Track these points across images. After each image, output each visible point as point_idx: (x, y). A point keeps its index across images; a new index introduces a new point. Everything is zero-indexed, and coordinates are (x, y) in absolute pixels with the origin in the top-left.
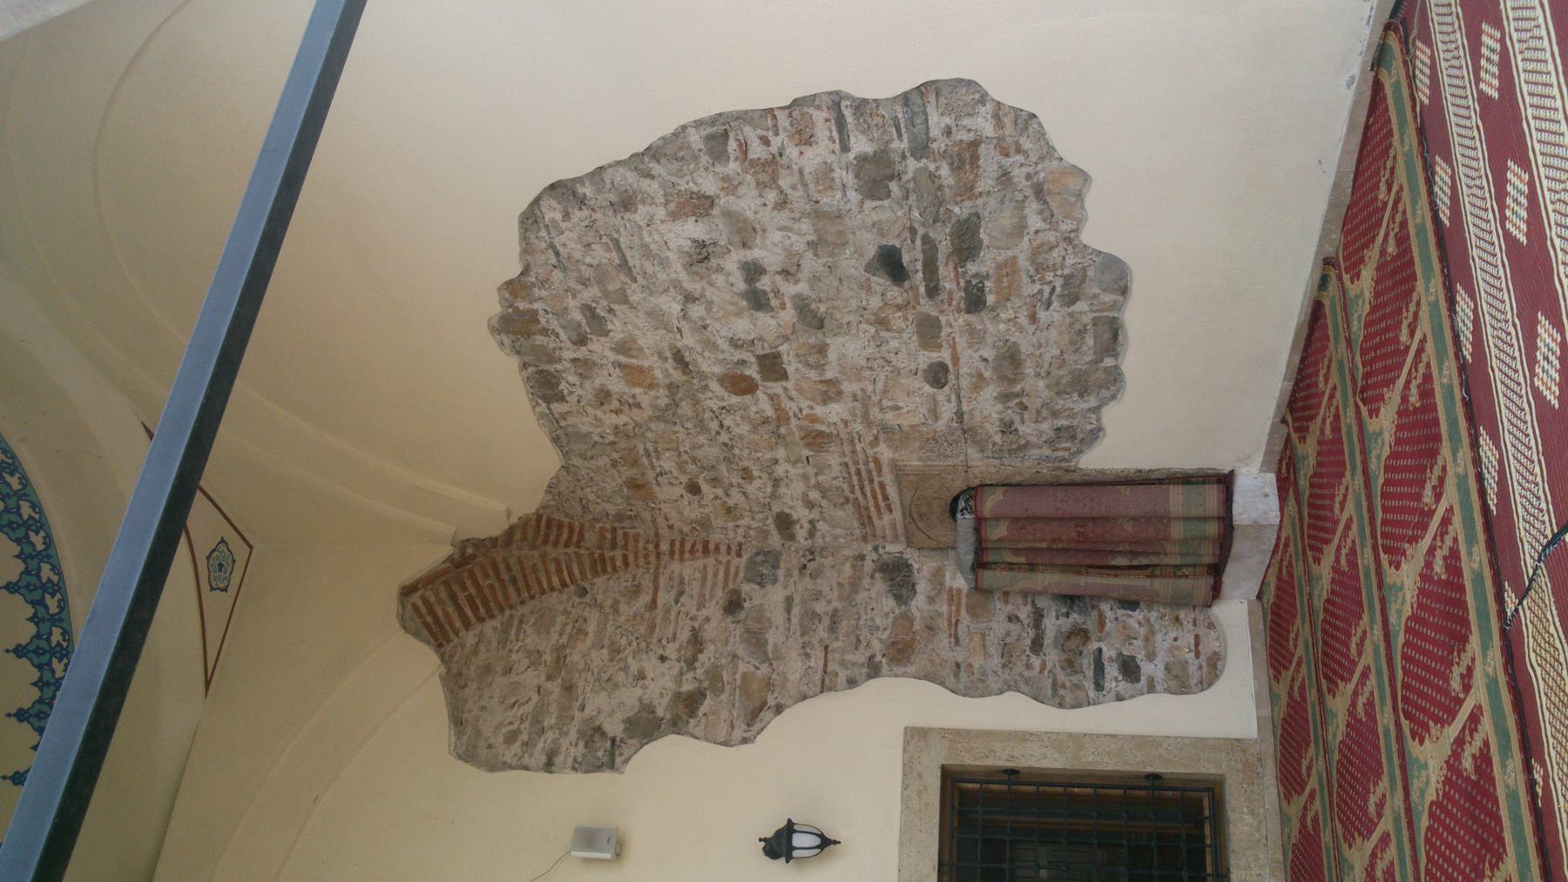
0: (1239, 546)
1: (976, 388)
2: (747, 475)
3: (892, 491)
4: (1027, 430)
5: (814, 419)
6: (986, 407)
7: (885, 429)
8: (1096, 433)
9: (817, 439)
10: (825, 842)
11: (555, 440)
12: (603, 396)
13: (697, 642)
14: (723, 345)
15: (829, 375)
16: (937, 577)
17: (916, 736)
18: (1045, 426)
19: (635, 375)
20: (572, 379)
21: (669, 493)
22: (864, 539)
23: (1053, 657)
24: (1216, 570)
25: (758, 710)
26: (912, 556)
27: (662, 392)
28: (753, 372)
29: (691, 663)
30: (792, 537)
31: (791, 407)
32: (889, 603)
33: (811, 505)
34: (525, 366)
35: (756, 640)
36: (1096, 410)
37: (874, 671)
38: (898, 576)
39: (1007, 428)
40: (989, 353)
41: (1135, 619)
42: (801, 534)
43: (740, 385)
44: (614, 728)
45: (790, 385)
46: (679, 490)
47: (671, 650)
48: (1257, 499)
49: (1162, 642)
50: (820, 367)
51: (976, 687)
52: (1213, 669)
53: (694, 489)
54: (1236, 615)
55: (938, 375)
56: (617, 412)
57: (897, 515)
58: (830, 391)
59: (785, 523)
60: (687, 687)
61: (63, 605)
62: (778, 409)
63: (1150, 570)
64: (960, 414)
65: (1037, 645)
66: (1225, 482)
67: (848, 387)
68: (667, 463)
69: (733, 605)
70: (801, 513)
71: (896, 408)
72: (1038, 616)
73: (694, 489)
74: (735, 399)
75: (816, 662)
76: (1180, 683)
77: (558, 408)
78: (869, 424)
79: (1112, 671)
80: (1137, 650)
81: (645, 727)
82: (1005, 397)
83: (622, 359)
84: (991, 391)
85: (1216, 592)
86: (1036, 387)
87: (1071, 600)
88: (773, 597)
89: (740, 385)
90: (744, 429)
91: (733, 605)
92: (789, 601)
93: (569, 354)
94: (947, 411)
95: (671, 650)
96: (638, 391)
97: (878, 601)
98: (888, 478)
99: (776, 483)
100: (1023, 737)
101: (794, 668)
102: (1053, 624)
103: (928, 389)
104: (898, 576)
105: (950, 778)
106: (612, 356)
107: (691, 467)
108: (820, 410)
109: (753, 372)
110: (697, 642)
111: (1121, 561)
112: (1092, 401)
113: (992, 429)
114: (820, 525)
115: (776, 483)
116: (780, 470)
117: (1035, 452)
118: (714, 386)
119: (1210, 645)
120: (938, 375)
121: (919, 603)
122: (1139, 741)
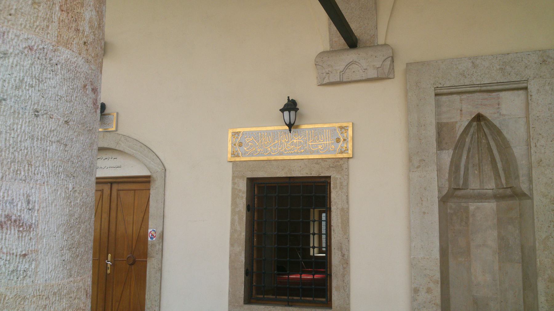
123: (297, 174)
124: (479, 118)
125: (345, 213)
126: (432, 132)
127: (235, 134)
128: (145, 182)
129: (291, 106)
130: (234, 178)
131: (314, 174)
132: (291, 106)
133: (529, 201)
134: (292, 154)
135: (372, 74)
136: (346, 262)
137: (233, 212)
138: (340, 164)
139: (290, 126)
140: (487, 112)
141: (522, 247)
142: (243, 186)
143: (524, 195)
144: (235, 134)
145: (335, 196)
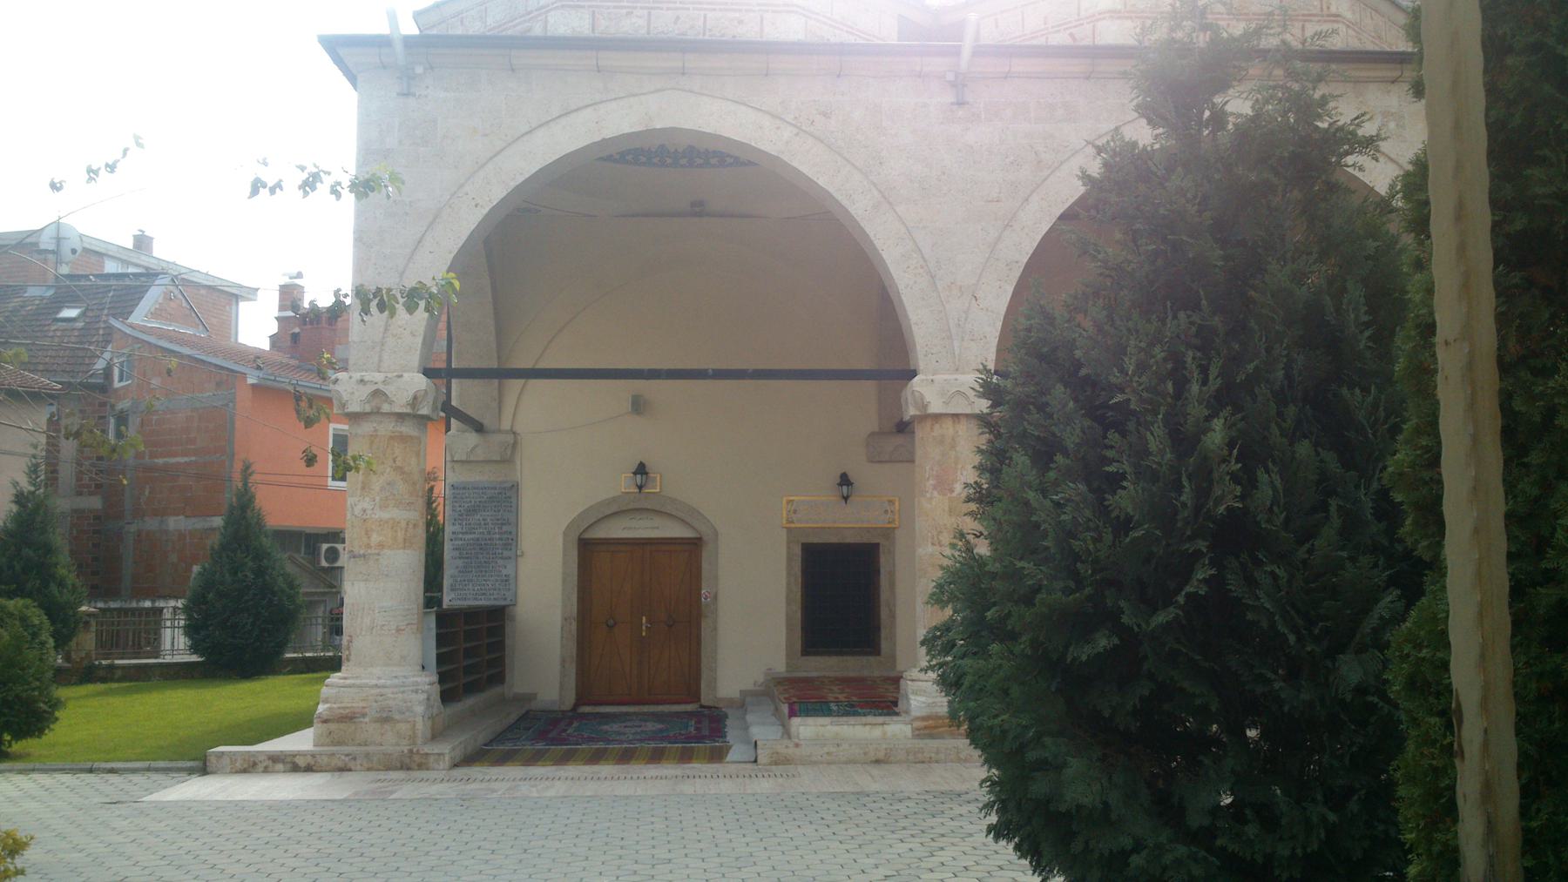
123: (850, 539)
125: (892, 574)
127: (789, 502)
128: (693, 547)
129: (845, 480)
130: (789, 543)
131: (865, 540)
132: (845, 480)
134: (844, 522)
136: (893, 616)
137: (789, 574)
138: (889, 533)
139: (846, 499)
142: (798, 550)
144: (789, 502)
145: (883, 560)
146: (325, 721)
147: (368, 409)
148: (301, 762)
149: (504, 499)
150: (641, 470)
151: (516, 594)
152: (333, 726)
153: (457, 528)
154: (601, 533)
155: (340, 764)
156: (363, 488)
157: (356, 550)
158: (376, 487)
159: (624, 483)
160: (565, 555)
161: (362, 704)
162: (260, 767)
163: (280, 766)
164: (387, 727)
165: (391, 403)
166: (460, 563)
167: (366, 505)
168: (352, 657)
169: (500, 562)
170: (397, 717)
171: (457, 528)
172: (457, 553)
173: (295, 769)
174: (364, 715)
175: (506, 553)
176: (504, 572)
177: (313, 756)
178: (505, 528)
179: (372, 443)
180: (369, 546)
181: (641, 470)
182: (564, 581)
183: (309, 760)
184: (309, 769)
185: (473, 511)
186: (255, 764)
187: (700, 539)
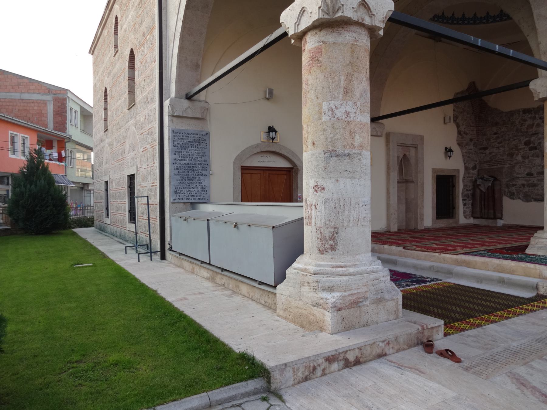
0: (490, 221)
1: (526, 180)
2: (499, 143)
3: (495, 167)
4: (514, 188)
5: (517, 155)
6: (520, 182)
7: (514, 166)
8: (514, 199)
9: (511, 155)
10: (450, 157)
11: (511, 111)
12: (525, 120)
13: (467, 134)
14: (539, 141)
15: (530, 158)
16: (474, 174)
17: (458, 171)
18: (515, 191)
19: (531, 126)
20: (530, 116)
21: (495, 129)
22: (480, 162)
23: (466, 193)
24: (481, 218)
25: (459, 144)
26: (476, 170)
27: (525, 130)
28: (531, 145)
29: (464, 133)
30: (481, 149)
31: (521, 151)
32: (472, 166)
33: (490, 153)
34: (534, 108)
35: (467, 144)
36: (520, 198)
37: (465, 164)
38: (474, 168)
39: (515, 185)
40: (536, 182)
41: (470, 206)
42: (481, 151)
43: (527, 143)
44: (458, 121)
45: (528, 151)
46: (495, 131)
47: (466, 130)
48: (500, 223)
49: (467, 210)
50: (533, 156)
51: (463, 181)
52: (466, 217)
53: (495, 134)
54: (471, 221)
55: (530, 174)
56: (519, 122)
57: (488, 168)
58: (524, 157)
59: (485, 149)
60: (462, 133)
61: (484, 23)
62: (520, 149)
63: (481, 208)
64: (518, 178)
65: (467, 190)
66: (501, 219)
67: (527, 161)
68: (503, 130)
69: (471, 140)
70: (488, 152)
71: (520, 168)
72: (470, 190)
73: (495, 134)
74: (523, 142)
75: (465, 154)
76: (464, 212)
77: (521, 113)
78: (516, 163)
79: (464, 202)
80: (467, 206)
81: (458, 126)
82: (523, 185)
83: (535, 125)
84: (525, 183)
85: (474, 218)
86: (527, 189)
87: (473, 195)
88: (472, 147)
89: (527, 143)
90: (514, 143)
91: (471, 140)
92: (471, 149)
93: (537, 116)
94: (520, 176)
95: (466, 130)
96: (526, 126)
97: (471, 165)
98: (499, 166)
99: (498, 148)
100: (459, 188)
101: (464, 151)
102: (470, 193)
103: (526, 173)
104: (474, 168)
105: (455, 176)
106: (536, 123)
107: (502, 134)
108: (520, 156)
109: (531, 145)
110: (467, 134)
111: (483, 203)
112: (522, 198)
113: (514, 183)
114: (484, 155)
115: (498, 148)
116: (502, 149)
117: (507, 190)
118: (527, 139)
119: (468, 217)
120: (530, 174)
121: (472, 171)
122: (459, 206)
124: (405, 155)
126: (396, 159)
133: (412, 184)
135: (379, 134)
140: (407, 153)
141: (406, 199)
143: (412, 182)
146: (339, 310)
147: (355, 19)
148: (351, 357)
149: (202, 141)
150: (271, 129)
151: (209, 197)
152: (344, 313)
153: (176, 157)
154: (248, 164)
155: (379, 351)
156: (346, 92)
157: (339, 150)
158: (357, 93)
159: (263, 137)
160: (234, 174)
161: (365, 289)
162: (319, 372)
163: (335, 366)
164: (381, 306)
165: (372, 16)
166: (179, 177)
167: (348, 109)
168: (339, 247)
169: (201, 178)
170: (387, 296)
171: (176, 157)
172: (176, 172)
173: (348, 364)
174: (366, 299)
175: (204, 173)
176: (204, 183)
177: (360, 349)
178: (203, 158)
179: (353, 52)
180: (353, 146)
181: (271, 129)
182: (234, 188)
183: (357, 353)
184: (357, 362)
185: (185, 146)
186: (315, 369)
187: (292, 168)
